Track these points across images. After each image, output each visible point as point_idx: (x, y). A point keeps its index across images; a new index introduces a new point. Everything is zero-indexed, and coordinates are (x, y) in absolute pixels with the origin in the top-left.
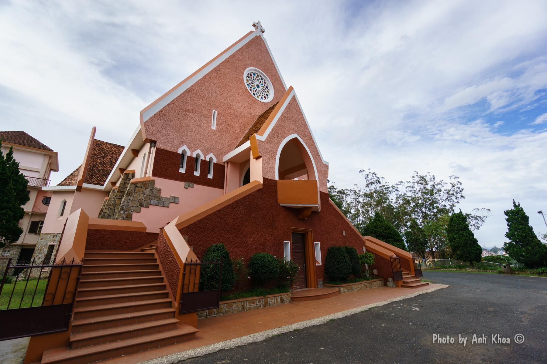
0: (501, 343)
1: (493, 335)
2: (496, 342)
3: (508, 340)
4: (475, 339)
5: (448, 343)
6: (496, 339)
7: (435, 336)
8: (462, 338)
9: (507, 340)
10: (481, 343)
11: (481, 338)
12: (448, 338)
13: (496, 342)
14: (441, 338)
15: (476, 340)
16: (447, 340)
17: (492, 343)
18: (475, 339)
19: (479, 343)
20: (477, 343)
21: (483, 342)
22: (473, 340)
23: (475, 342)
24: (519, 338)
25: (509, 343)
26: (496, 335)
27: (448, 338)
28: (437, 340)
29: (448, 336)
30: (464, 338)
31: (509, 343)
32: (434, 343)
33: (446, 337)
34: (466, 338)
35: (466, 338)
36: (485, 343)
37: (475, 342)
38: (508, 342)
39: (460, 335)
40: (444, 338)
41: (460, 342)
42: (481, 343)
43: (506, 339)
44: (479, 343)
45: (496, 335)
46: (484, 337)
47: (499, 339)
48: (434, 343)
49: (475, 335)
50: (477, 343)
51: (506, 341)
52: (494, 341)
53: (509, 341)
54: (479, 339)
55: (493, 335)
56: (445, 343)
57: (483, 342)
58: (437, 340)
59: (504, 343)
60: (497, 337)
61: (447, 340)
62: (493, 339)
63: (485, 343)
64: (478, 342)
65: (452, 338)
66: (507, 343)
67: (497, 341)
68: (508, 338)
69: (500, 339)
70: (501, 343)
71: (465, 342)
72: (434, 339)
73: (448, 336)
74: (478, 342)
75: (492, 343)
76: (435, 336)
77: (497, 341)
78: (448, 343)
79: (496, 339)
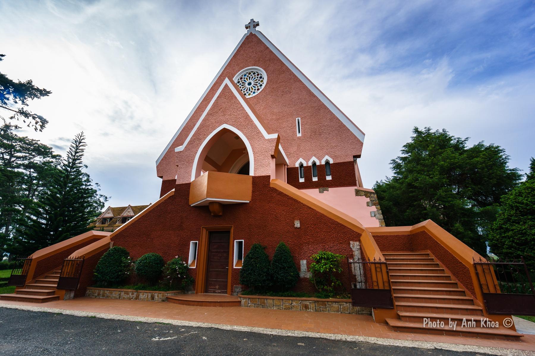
0: (490, 327)
2: (485, 326)
3: (497, 324)
4: (464, 323)
7: (426, 320)
8: (452, 322)
9: (496, 323)
11: (470, 322)
13: (485, 326)
14: (431, 322)
15: (465, 324)
17: (482, 326)
18: (464, 323)
25: (498, 326)
30: (454, 322)
31: (498, 326)
34: (456, 322)
35: (456, 322)
38: (497, 326)
43: (495, 323)
51: (495, 324)
52: (483, 325)
53: (498, 325)
54: (469, 323)
57: (473, 326)
59: (493, 327)
61: (437, 324)
66: (496, 327)
67: (486, 325)
68: (497, 322)
70: (490, 327)
75: (482, 326)
76: (426, 320)
77: (486, 325)
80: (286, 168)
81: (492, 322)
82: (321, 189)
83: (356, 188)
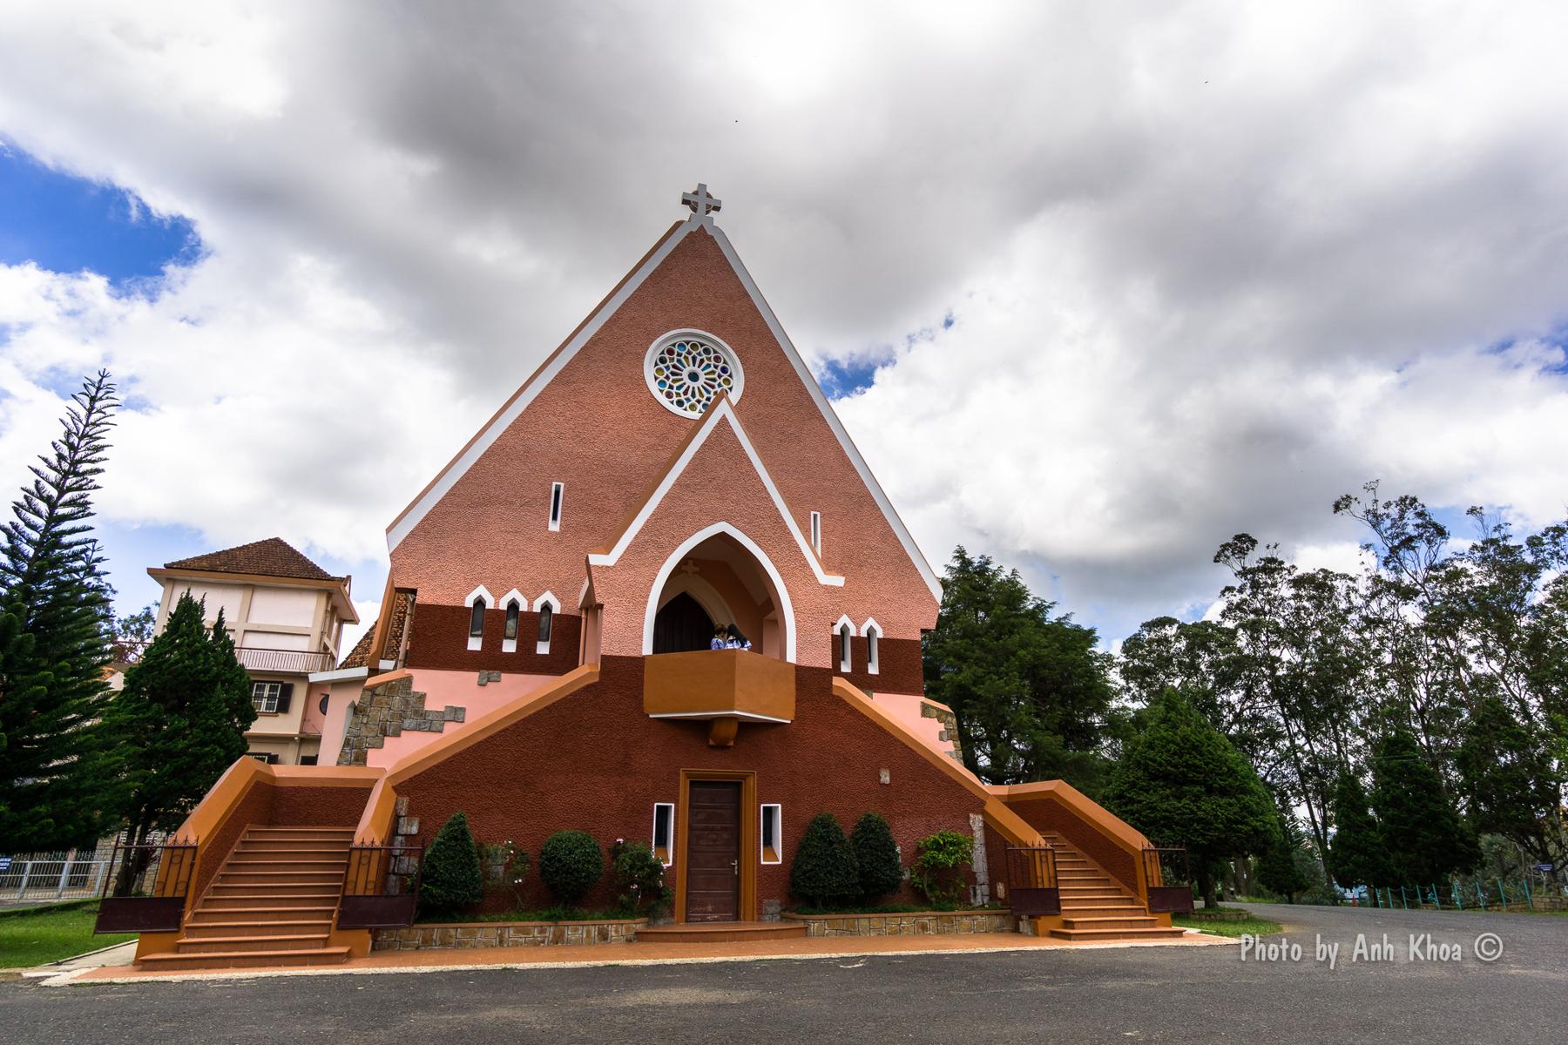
4: (1361, 948)
10: (1379, 958)
15: (1364, 951)
18: (1361, 948)
19: (1373, 959)
20: (1366, 958)
21: (1385, 958)
22: (1357, 951)
23: (1360, 956)
35: (1336, 945)
37: (1360, 956)
42: (1379, 958)
44: (1373, 959)
54: (1373, 948)
57: (1385, 958)
64: (1370, 956)
74: (1370, 956)
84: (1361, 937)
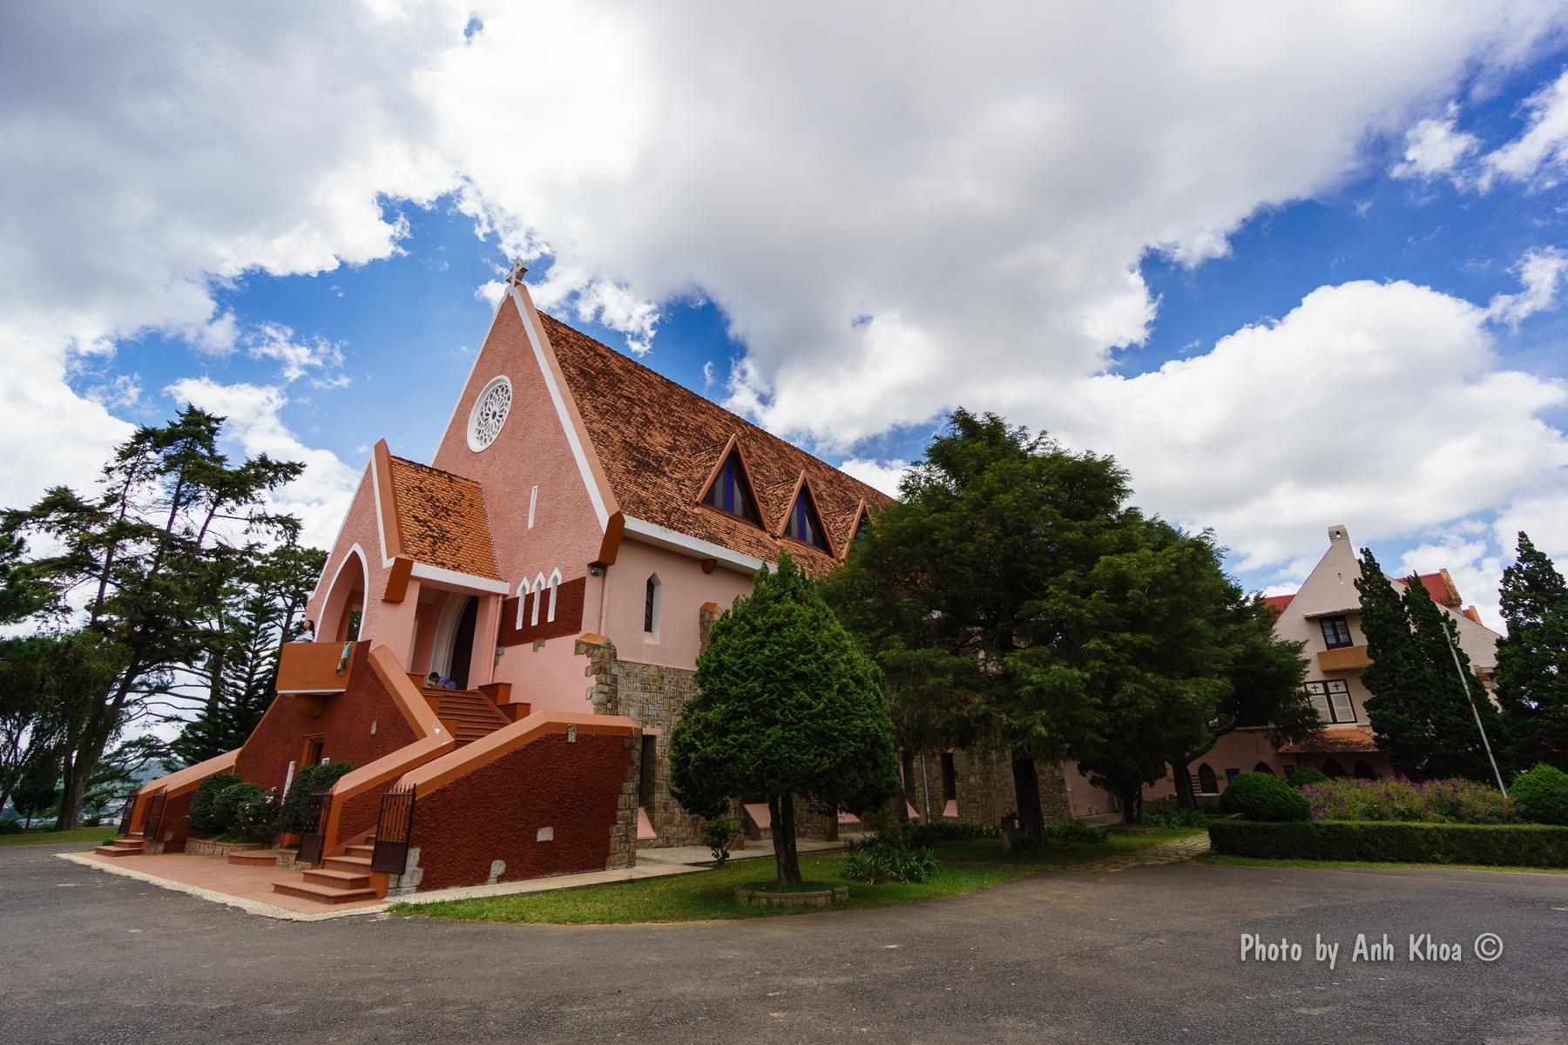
1: (1412, 937)
2: (1422, 958)
3: (1456, 950)
4: (1361, 947)
5: (1284, 958)
6: (1423, 947)
7: (1247, 941)
8: (1324, 946)
9: (1454, 949)
10: (1379, 958)
11: (1378, 946)
12: (1284, 946)
13: (1422, 958)
14: (1263, 947)
15: (1364, 951)
16: (1280, 951)
17: (1412, 958)
18: (1361, 947)
19: (1373, 959)
20: (1366, 958)
21: (1385, 958)
22: (1357, 951)
23: (1361, 956)
24: (1489, 946)
25: (1459, 959)
26: (1422, 936)
27: (1284, 946)
28: (1251, 953)
29: (1284, 941)
30: (1330, 946)
31: (1459, 959)
32: (1243, 958)
33: (1279, 944)
34: (1336, 945)
35: (1336, 945)
36: (1391, 959)
37: (1361, 956)
39: (1318, 936)
40: (1272, 946)
41: (1318, 958)
42: (1379, 958)
44: (1373, 959)
45: (1422, 936)
46: (1388, 943)
47: (1430, 947)
48: (1243, 958)
49: (1361, 938)
50: (1366, 958)
51: (1452, 953)
53: (1459, 953)
54: (1373, 948)
55: (1412, 937)
56: (1274, 959)
57: (1385, 958)
58: (1251, 953)
59: (1446, 959)
60: (1424, 943)
61: (1280, 951)
62: (1414, 948)
63: (1391, 959)
64: (1370, 957)
65: (1295, 946)
66: (1454, 959)
67: (1425, 954)
68: (1456, 946)
69: (1435, 946)
71: (1333, 957)
72: (1244, 949)
73: (1284, 941)
74: (1370, 957)
75: (1412, 958)
76: (1247, 941)
77: (1425, 954)
78: (1284, 958)
79: (1423, 947)
80: (500, 603)
81: (1443, 946)
82: (538, 641)
83: (577, 637)
84: (1361, 938)
